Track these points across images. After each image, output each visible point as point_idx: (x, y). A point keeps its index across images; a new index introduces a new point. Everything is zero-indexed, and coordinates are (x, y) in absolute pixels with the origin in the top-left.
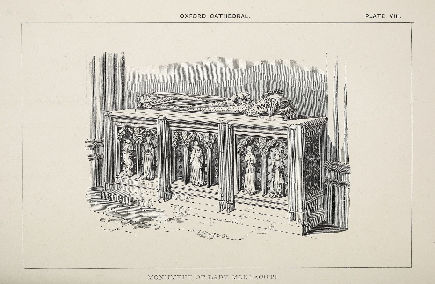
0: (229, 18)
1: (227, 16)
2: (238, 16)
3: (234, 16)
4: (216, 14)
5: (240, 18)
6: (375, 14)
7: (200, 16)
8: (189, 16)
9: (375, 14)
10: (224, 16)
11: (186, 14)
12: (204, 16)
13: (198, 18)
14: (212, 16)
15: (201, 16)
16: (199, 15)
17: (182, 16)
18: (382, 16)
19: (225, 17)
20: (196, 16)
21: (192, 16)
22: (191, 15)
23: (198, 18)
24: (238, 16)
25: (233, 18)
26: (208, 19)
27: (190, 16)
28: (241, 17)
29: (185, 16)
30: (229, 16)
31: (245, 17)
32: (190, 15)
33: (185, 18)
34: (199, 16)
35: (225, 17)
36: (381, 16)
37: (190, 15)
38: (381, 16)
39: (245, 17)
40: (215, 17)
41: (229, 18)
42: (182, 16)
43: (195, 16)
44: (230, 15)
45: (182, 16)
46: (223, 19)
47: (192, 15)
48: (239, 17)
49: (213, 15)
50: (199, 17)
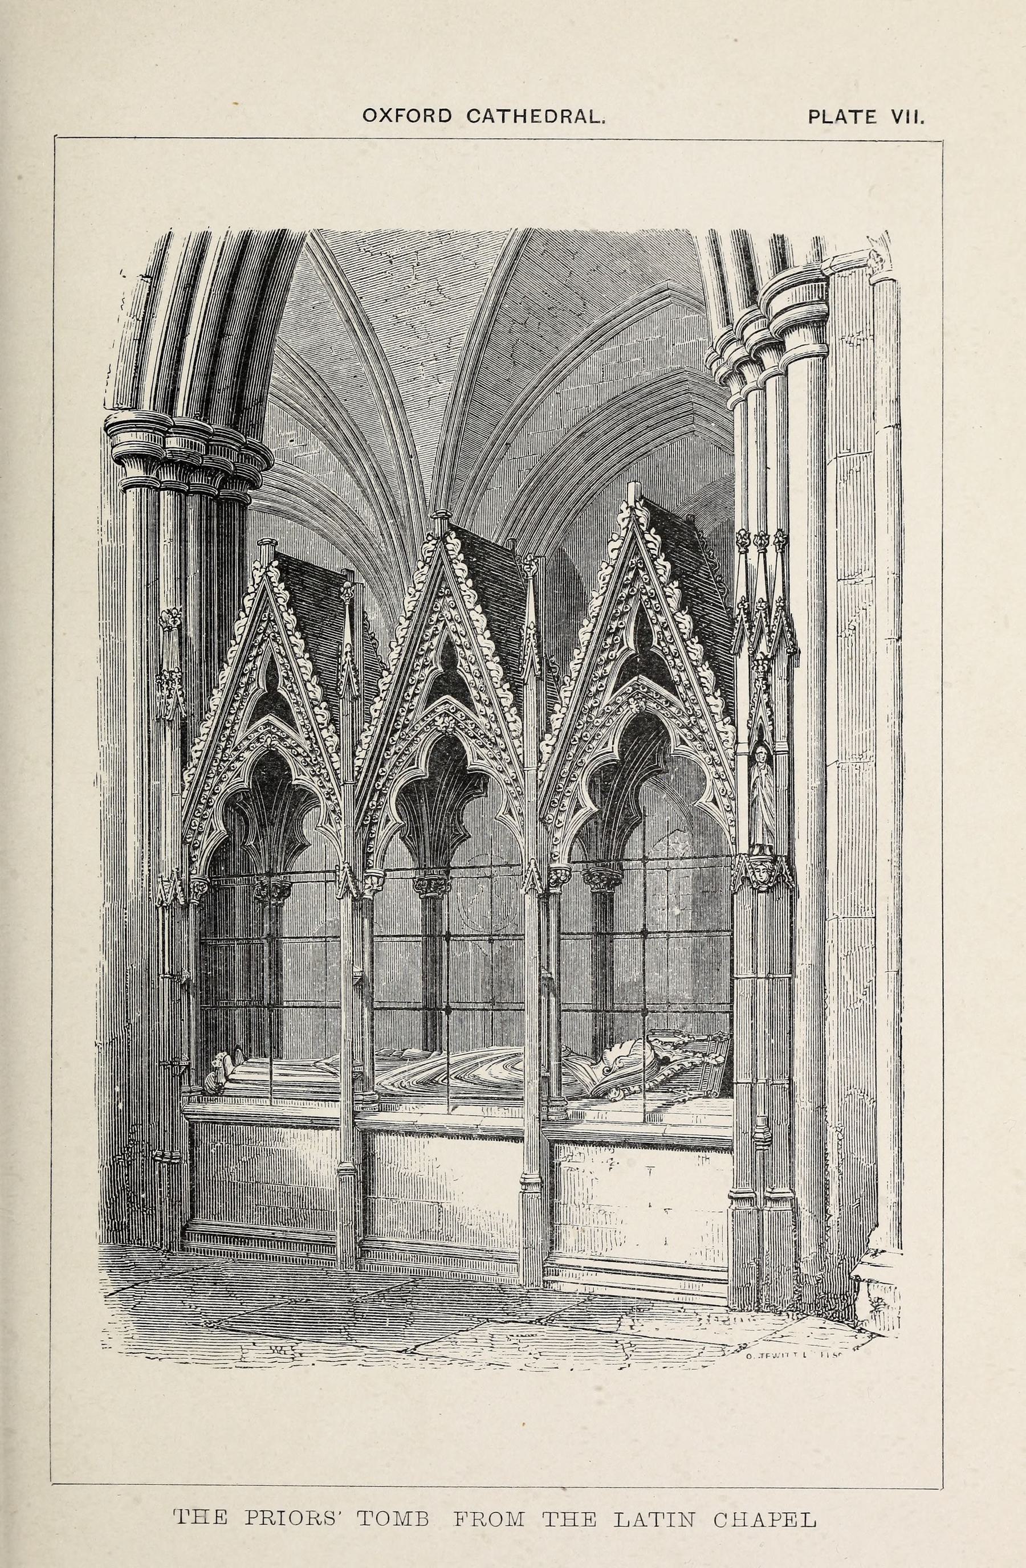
0: (532, 122)
1: (524, 116)
2: (565, 115)
3: (551, 116)
4: (488, 110)
5: (570, 121)
6: (841, 111)
7: (433, 113)
8: (392, 115)
9: (841, 111)
10: (516, 116)
11: (382, 109)
12: (445, 115)
13: (425, 121)
14: (474, 116)
15: (436, 117)
16: (429, 113)
17: (368, 115)
18: (868, 117)
19: (520, 120)
20: (419, 117)
21: (405, 115)
22: (400, 113)
23: (425, 121)
24: (565, 115)
25: (547, 121)
26: (459, 125)
27: (398, 116)
28: (573, 118)
29: (380, 115)
30: (533, 116)
31: (588, 119)
32: (397, 110)
33: (381, 121)
34: (428, 114)
35: (520, 120)
36: (861, 117)
37: (397, 110)
38: (861, 117)
39: (588, 119)
40: (485, 118)
41: (532, 122)
42: (368, 115)
43: (413, 116)
44: (535, 113)
45: (370, 115)
46: (510, 128)
47: (404, 113)
48: (566, 120)
49: (479, 113)
50: (428, 119)
